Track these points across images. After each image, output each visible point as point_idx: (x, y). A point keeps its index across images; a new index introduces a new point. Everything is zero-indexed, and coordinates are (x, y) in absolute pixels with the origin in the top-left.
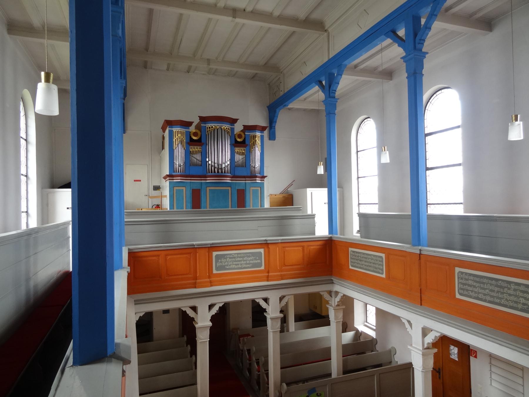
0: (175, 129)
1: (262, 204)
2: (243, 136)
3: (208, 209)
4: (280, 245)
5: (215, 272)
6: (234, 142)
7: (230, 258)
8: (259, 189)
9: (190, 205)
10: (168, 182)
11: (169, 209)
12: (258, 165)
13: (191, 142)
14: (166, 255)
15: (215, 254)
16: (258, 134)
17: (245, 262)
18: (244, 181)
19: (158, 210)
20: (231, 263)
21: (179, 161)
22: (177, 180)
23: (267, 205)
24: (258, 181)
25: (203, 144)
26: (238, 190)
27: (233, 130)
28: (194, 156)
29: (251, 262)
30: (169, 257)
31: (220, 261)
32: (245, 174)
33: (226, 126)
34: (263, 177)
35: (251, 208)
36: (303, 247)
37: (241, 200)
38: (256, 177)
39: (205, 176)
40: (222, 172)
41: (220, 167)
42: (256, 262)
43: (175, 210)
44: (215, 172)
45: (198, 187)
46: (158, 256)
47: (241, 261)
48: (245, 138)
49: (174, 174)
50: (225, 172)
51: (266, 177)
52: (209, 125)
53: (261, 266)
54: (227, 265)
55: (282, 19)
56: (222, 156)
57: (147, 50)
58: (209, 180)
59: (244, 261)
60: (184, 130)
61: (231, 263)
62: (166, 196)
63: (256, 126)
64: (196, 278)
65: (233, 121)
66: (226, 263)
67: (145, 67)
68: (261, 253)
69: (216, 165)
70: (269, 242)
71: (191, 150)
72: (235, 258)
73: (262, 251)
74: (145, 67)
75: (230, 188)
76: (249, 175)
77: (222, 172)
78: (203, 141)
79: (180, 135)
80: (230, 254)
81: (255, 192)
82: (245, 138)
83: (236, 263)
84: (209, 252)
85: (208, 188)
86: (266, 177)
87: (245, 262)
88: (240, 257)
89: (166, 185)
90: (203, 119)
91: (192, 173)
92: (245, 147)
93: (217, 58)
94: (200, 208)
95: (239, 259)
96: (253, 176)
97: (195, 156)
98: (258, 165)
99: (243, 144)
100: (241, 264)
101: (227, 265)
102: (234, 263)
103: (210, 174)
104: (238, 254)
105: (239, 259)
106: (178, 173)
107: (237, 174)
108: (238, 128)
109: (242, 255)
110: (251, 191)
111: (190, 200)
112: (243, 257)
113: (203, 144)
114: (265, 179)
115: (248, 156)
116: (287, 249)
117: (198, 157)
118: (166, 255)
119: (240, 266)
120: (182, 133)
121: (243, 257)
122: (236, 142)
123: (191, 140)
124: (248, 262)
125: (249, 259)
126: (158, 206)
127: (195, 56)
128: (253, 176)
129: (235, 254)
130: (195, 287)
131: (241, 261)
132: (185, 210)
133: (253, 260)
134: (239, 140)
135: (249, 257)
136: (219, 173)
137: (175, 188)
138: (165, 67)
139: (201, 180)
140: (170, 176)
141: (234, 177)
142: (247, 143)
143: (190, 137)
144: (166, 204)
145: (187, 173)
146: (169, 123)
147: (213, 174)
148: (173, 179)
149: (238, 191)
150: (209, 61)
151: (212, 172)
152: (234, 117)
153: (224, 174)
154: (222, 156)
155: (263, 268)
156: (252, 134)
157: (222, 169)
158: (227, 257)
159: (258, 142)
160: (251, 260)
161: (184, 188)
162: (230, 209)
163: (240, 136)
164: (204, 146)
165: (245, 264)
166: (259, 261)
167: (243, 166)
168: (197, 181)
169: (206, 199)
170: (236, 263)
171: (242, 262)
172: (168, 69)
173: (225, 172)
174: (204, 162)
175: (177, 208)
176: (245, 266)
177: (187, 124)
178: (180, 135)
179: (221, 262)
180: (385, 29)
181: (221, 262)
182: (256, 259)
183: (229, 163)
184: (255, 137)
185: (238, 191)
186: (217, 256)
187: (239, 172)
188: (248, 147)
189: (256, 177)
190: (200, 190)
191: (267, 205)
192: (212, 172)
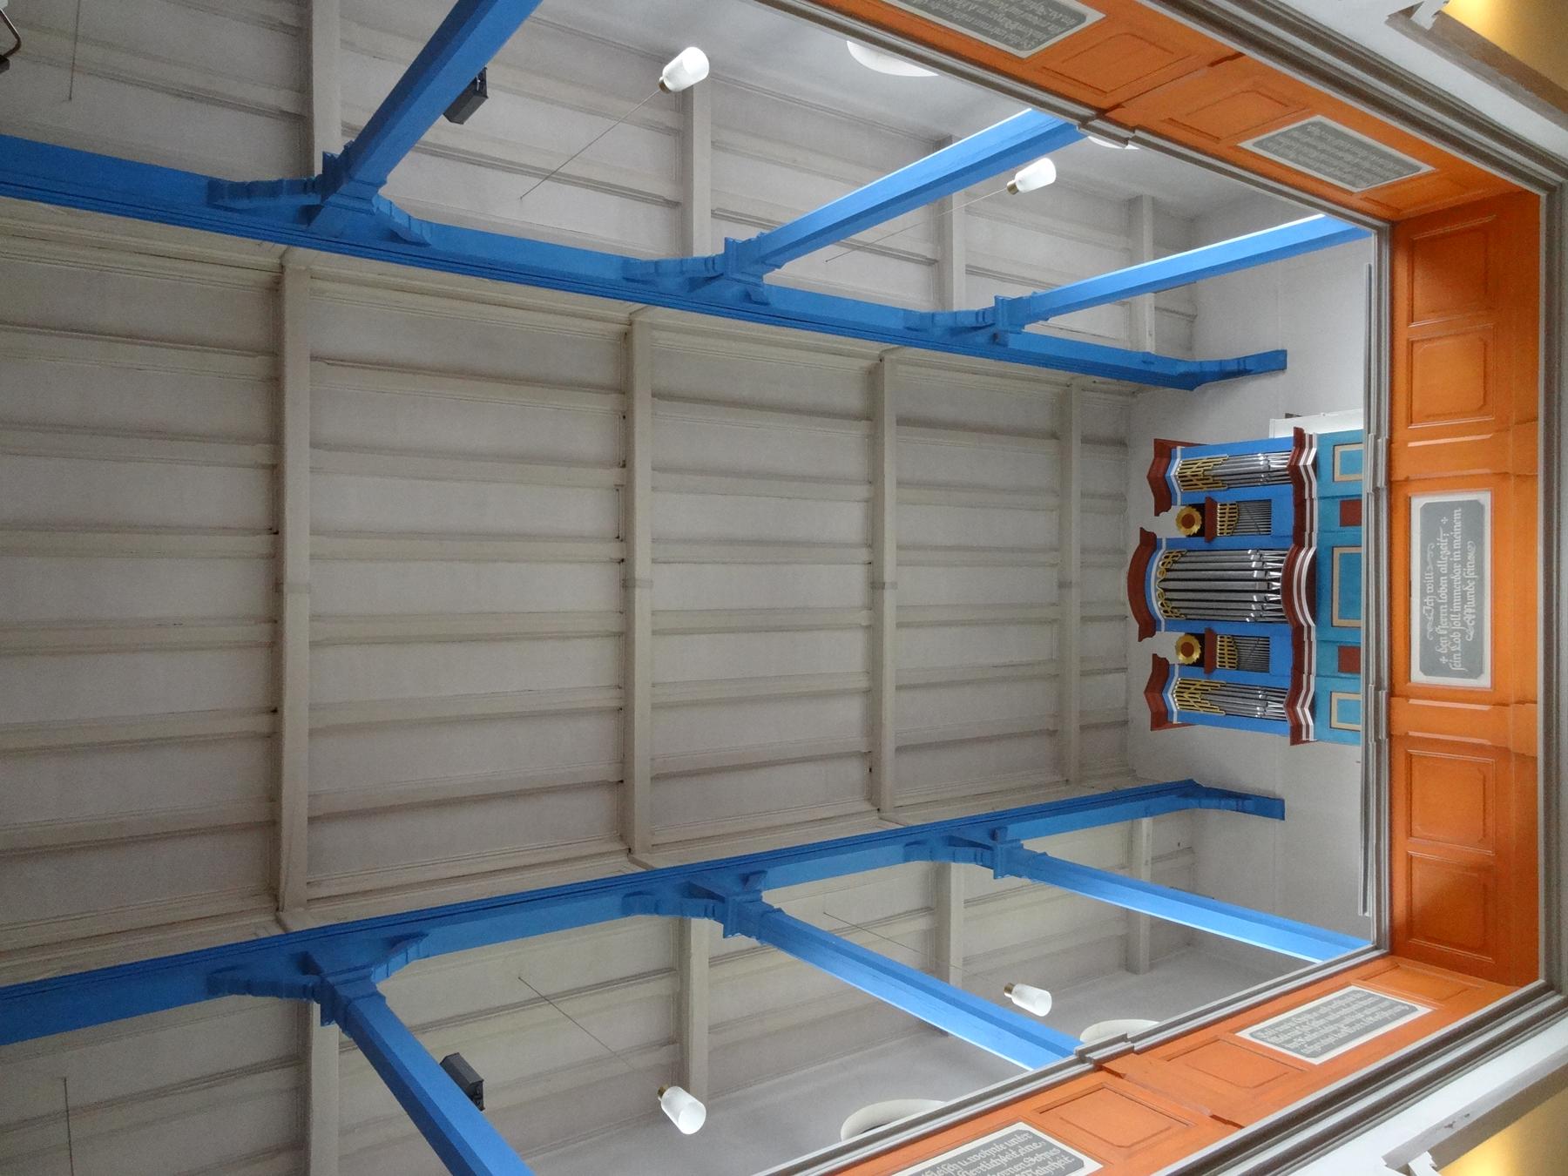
4: (1397, 436)
5: (1484, 681)
6: (1201, 540)
7: (1436, 622)
8: (1339, 450)
14: (1410, 833)
15: (1417, 676)
16: (1175, 469)
17: (1457, 568)
18: (1316, 503)
20: (1456, 619)
22: (1304, 713)
24: (1307, 459)
25: (1210, 630)
27: (1172, 543)
29: (1457, 544)
30: (1416, 827)
31: (1443, 660)
34: (1300, 438)
36: (1411, 344)
39: (1298, 630)
40: (1276, 580)
41: (1263, 586)
42: (1458, 524)
44: (1277, 602)
45: (1333, 652)
46: (1410, 859)
47: (1450, 582)
48: (1194, 506)
49: (1289, 724)
51: (1299, 433)
53: (1478, 506)
54: (1463, 633)
55: (874, 479)
57: (1052, 733)
58: (1305, 617)
59: (1450, 570)
61: (1456, 619)
64: (1502, 752)
65: (1149, 542)
66: (1456, 637)
67: (1126, 723)
68: (1426, 509)
70: (1382, 482)
72: (1437, 607)
73: (1418, 503)
74: (1126, 723)
75: (1337, 552)
78: (1200, 628)
80: (1424, 620)
82: (1194, 506)
83: (1457, 599)
84: (1407, 697)
85: (1336, 622)
87: (1457, 568)
88: (1437, 585)
90: (1148, 627)
93: (1053, 565)
95: (1443, 591)
96: (1294, 475)
99: (1205, 509)
100: (1464, 581)
101: (1463, 633)
102: (1457, 608)
104: (1423, 594)
105: (1443, 591)
109: (1430, 577)
110: (1346, 478)
112: (1438, 575)
114: (1307, 432)
116: (1416, 406)
118: (1410, 833)
119: (1470, 588)
121: (1438, 575)
122: (1200, 533)
124: (1457, 558)
125: (1445, 550)
127: (1055, 621)
128: (1294, 475)
129: (1423, 604)
130: (1535, 759)
131: (1450, 582)
133: (1451, 540)
135: (1437, 549)
137: (1335, 723)
138: (1122, 676)
141: (1299, 541)
143: (1194, 664)
145: (1287, 684)
146: (1161, 719)
150: (1063, 585)
155: (1485, 498)
156: (1175, 484)
158: (1433, 633)
160: (1451, 543)
161: (1335, 697)
163: (1186, 521)
164: (1217, 628)
165: (1464, 566)
166: (1457, 514)
168: (1314, 656)
170: (1457, 599)
171: (1456, 578)
172: (1124, 670)
176: (1471, 568)
177: (1161, 669)
179: (1450, 655)
180: (756, 306)
181: (1450, 655)
182: (1449, 528)
186: (1426, 670)
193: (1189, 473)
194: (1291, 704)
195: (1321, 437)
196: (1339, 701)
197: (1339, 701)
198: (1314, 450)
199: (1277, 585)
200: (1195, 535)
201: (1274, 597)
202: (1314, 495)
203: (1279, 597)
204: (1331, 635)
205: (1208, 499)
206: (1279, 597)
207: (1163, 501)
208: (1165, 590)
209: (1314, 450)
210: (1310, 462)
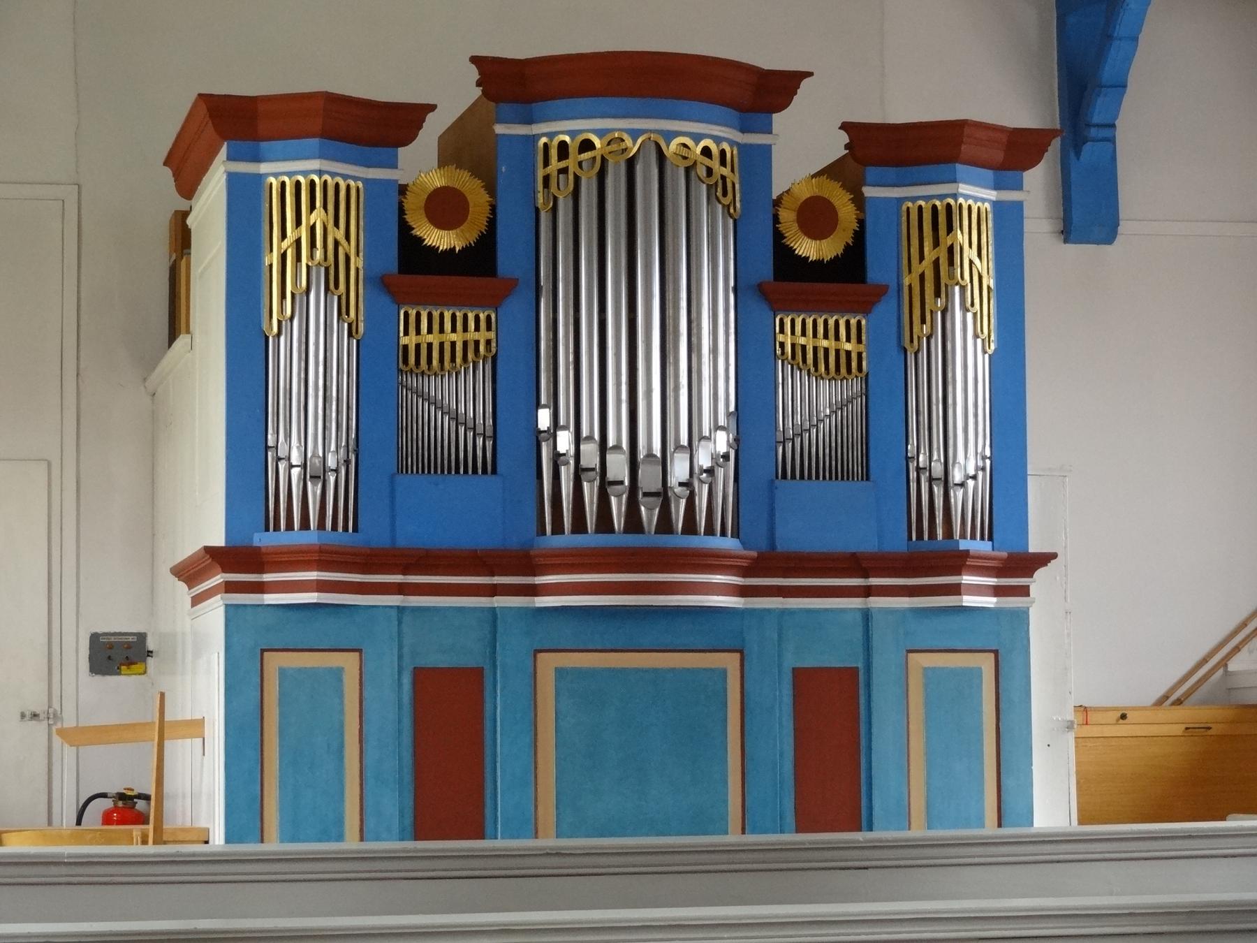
0: (286, 169)
1: (1010, 800)
2: (846, 212)
3: (549, 841)
8: (986, 663)
9: (394, 803)
10: (214, 613)
11: (218, 838)
12: (969, 458)
13: (414, 271)
16: (975, 194)
18: (855, 603)
19: (131, 845)
21: (309, 438)
23: (1052, 805)
25: (510, 286)
26: (803, 678)
27: (756, 163)
28: (432, 386)
32: (860, 538)
33: (696, 135)
34: (1024, 564)
35: (918, 831)
37: (829, 760)
38: (958, 562)
39: (526, 562)
41: (649, 478)
43: (273, 845)
48: (860, 235)
49: (264, 540)
50: (690, 526)
51: (1044, 559)
52: (560, 129)
56: (666, 383)
60: (350, 174)
62: (195, 727)
63: (960, 125)
69: (618, 467)
71: (410, 340)
75: (731, 662)
76: (897, 542)
77: (665, 524)
79: (318, 217)
81: (951, 694)
82: (860, 235)
85: (549, 663)
86: (1044, 559)
89: (199, 632)
91: (414, 533)
92: (865, 305)
94: (478, 833)
97: (444, 389)
98: (969, 458)
99: (845, 280)
103: (568, 540)
106: (297, 538)
107: (796, 535)
108: (802, 145)
111: (395, 758)
113: (510, 286)
114: (1040, 581)
115: (891, 392)
117: (463, 397)
120: (335, 201)
122: (788, 264)
123: (414, 255)
126: (128, 809)
132: (351, 843)
134: (807, 248)
136: (641, 536)
137: (275, 661)
139: (493, 591)
140: (236, 560)
142: (875, 273)
143: (405, 229)
144: (199, 788)
145: (375, 534)
146: (233, 121)
147: (592, 539)
148: (260, 588)
149: (807, 683)
151: (579, 525)
152: (769, 57)
153: (679, 541)
154: (666, 383)
156: (921, 194)
157: (664, 495)
159: (977, 261)
161: (349, 662)
162: (733, 837)
167: (846, 475)
169: (531, 750)
173: (690, 526)
174: (508, 448)
175: (291, 835)
178: (318, 217)
183: (722, 442)
184: (945, 219)
185: (807, 683)
187: (810, 521)
188: (884, 309)
189: (958, 562)
190: (477, 673)
191: (1052, 805)
192: (579, 525)
193: (961, 237)
194: (325, 558)
195: (1021, 617)
196: (338, 673)
197: (338, 673)
198: (990, 602)
199: (649, 514)
200: (778, 236)
201: (617, 507)
202: (876, 602)
203: (618, 521)
204: (512, 647)
205: (880, 292)
206: (618, 521)
207: (879, 148)
208: (631, 163)
209: (990, 602)
210: (969, 600)
